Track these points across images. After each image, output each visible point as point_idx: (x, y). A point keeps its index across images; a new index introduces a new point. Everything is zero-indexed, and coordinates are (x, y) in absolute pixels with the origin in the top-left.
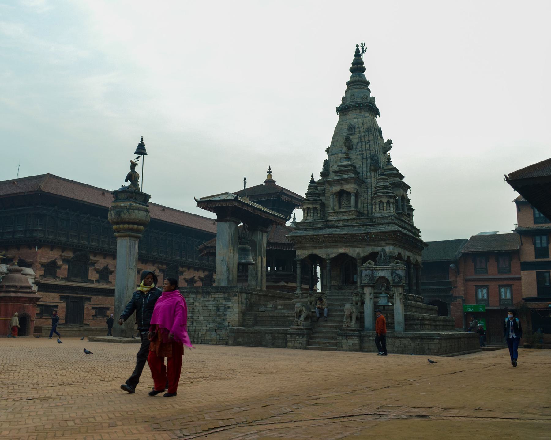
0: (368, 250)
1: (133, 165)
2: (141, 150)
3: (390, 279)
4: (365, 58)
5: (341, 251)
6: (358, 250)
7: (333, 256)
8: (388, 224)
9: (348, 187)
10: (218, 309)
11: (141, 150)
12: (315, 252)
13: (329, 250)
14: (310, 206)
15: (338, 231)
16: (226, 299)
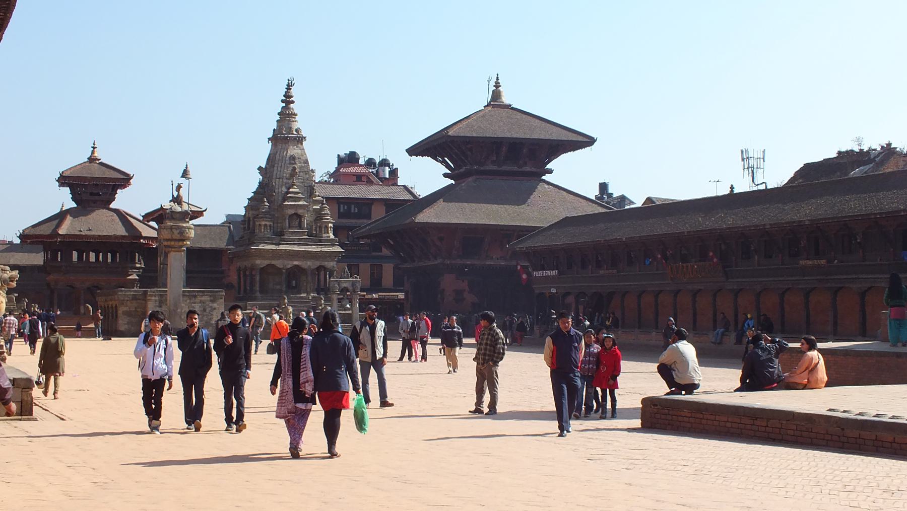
0: (317, 264)
1: (179, 187)
2: (185, 174)
3: (351, 288)
4: (293, 91)
5: (296, 263)
6: (309, 263)
7: (289, 267)
8: (334, 245)
9: (300, 212)
10: (205, 310)
11: (185, 174)
12: (273, 262)
13: (286, 262)
14: (268, 223)
15: (296, 248)
16: (212, 301)
